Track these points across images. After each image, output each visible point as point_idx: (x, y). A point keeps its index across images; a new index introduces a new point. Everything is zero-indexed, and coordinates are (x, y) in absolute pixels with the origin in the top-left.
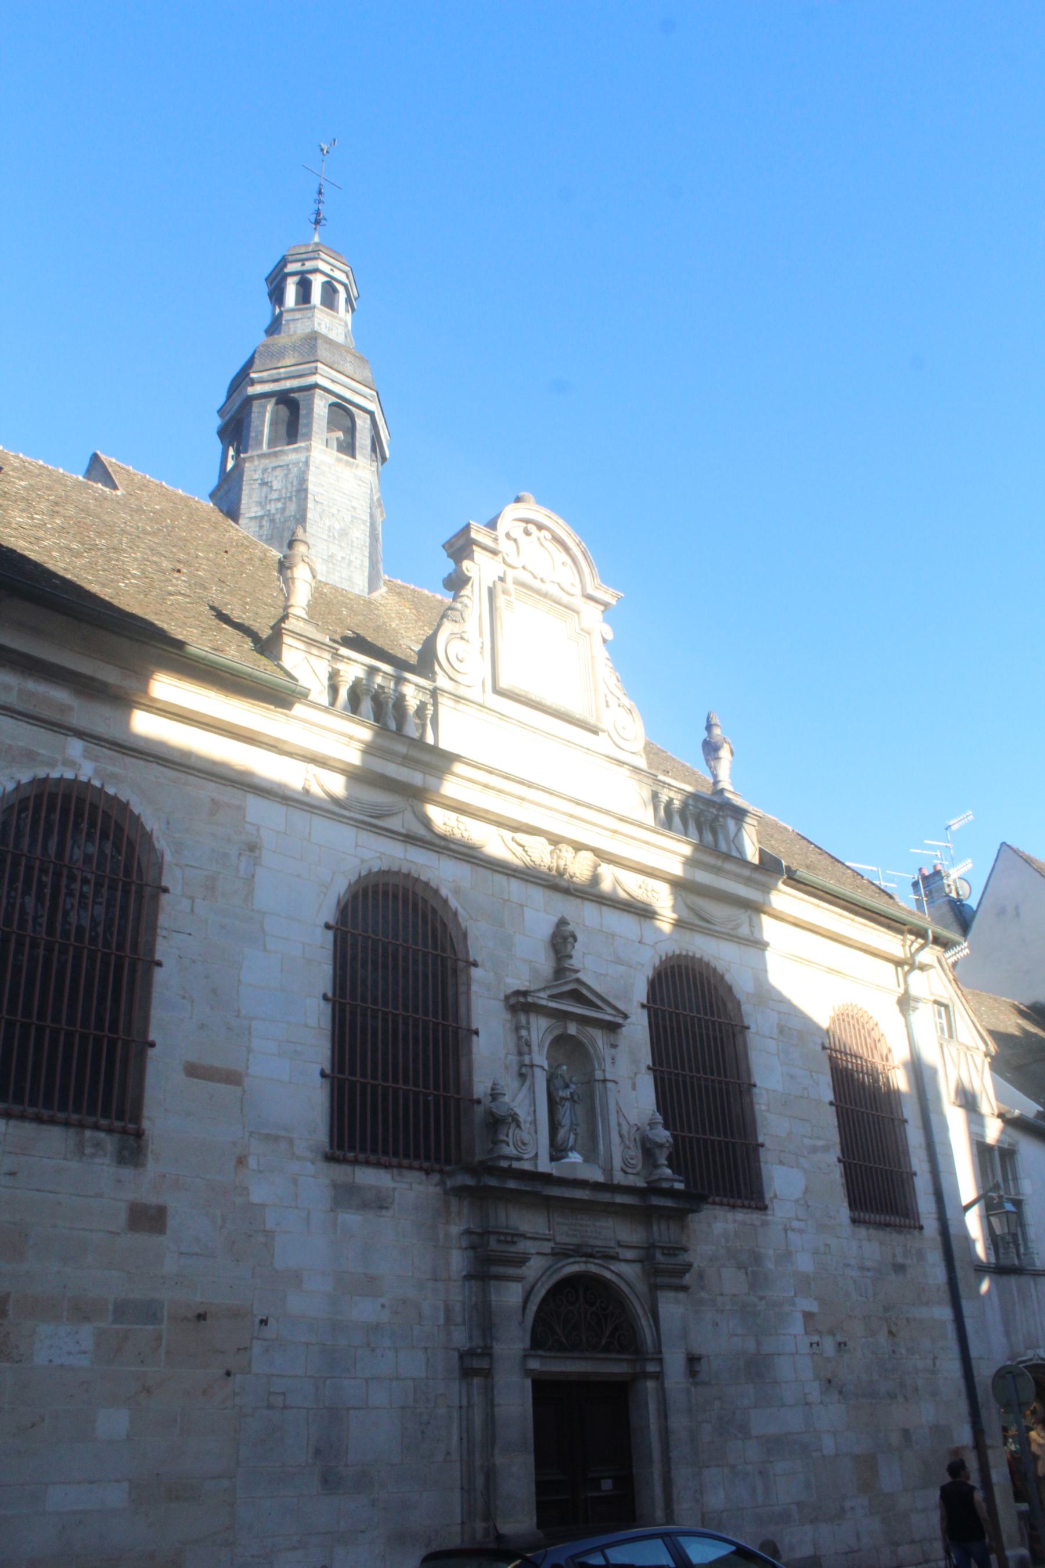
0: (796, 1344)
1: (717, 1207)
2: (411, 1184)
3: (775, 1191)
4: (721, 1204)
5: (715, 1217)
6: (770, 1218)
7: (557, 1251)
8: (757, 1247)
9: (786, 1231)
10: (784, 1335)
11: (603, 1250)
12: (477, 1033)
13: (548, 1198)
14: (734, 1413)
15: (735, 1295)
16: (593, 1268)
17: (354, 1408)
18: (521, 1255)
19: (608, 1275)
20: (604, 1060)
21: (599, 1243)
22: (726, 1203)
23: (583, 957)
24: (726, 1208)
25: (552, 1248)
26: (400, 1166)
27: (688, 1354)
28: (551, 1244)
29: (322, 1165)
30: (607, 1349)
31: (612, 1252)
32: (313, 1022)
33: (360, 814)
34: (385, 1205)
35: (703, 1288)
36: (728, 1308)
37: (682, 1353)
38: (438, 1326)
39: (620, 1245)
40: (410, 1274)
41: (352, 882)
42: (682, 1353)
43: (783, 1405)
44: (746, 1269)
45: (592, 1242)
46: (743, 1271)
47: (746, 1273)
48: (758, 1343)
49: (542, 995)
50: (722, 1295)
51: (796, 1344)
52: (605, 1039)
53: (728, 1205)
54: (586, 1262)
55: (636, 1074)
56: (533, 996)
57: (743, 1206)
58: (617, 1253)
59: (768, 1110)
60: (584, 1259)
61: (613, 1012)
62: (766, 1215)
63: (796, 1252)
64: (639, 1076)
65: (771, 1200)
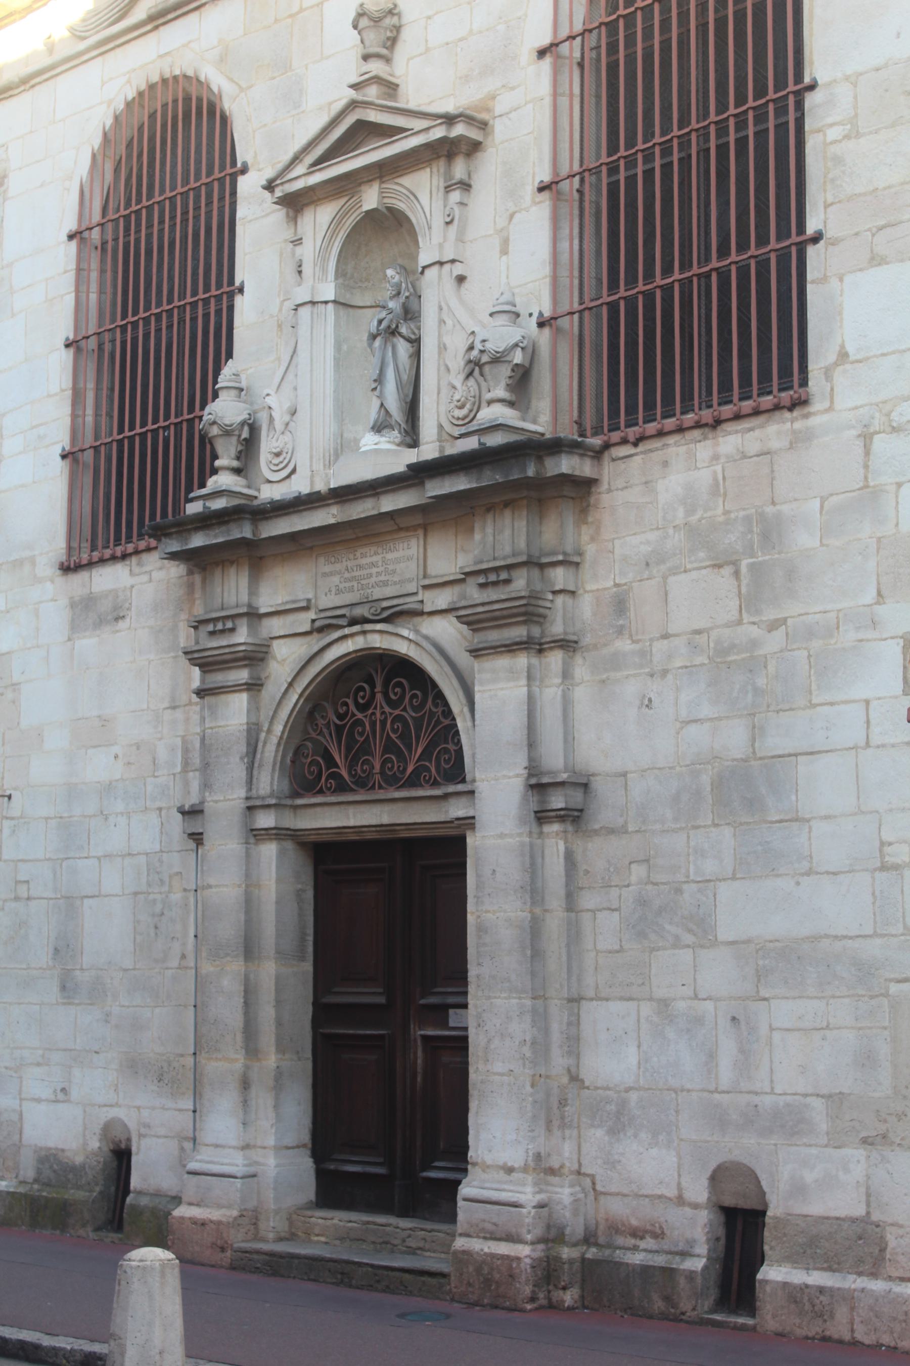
0: (868, 722)
1: (671, 440)
2: (150, 572)
3: (842, 346)
4: (680, 430)
5: (665, 464)
6: (814, 421)
7: (318, 624)
8: (773, 503)
9: (867, 438)
10: (832, 704)
11: (395, 602)
12: (241, 290)
13: (294, 537)
14: (679, 891)
15: (698, 632)
16: (377, 641)
17: (87, 897)
18: (227, 650)
19: (402, 648)
20: (430, 228)
21: (389, 591)
22: (710, 421)
23: (426, 28)
24: (696, 433)
25: (313, 621)
26: (137, 552)
27: (530, 775)
28: (312, 615)
29: (60, 580)
30: (413, 782)
31: (410, 603)
32: (55, 388)
33: (98, 32)
34: (121, 615)
35: (620, 631)
36: (678, 663)
37: (517, 776)
38: (174, 775)
39: (425, 587)
40: (145, 706)
41: (96, 147)
42: (517, 776)
43: (809, 873)
44: (735, 563)
45: (377, 593)
46: (727, 571)
47: (737, 574)
48: (756, 733)
49: (300, 169)
50: (666, 636)
51: (868, 722)
52: (435, 182)
53: (698, 425)
54: (364, 633)
55: (512, 216)
56: (282, 184)
57: (737, 417)
58: (422, 602)
59: (854, 134)
60: (356, 628)
61: (425, 124)
62: (806, 416)
63: (899, 485)
64: (517, 216)
65: (828, 373)
